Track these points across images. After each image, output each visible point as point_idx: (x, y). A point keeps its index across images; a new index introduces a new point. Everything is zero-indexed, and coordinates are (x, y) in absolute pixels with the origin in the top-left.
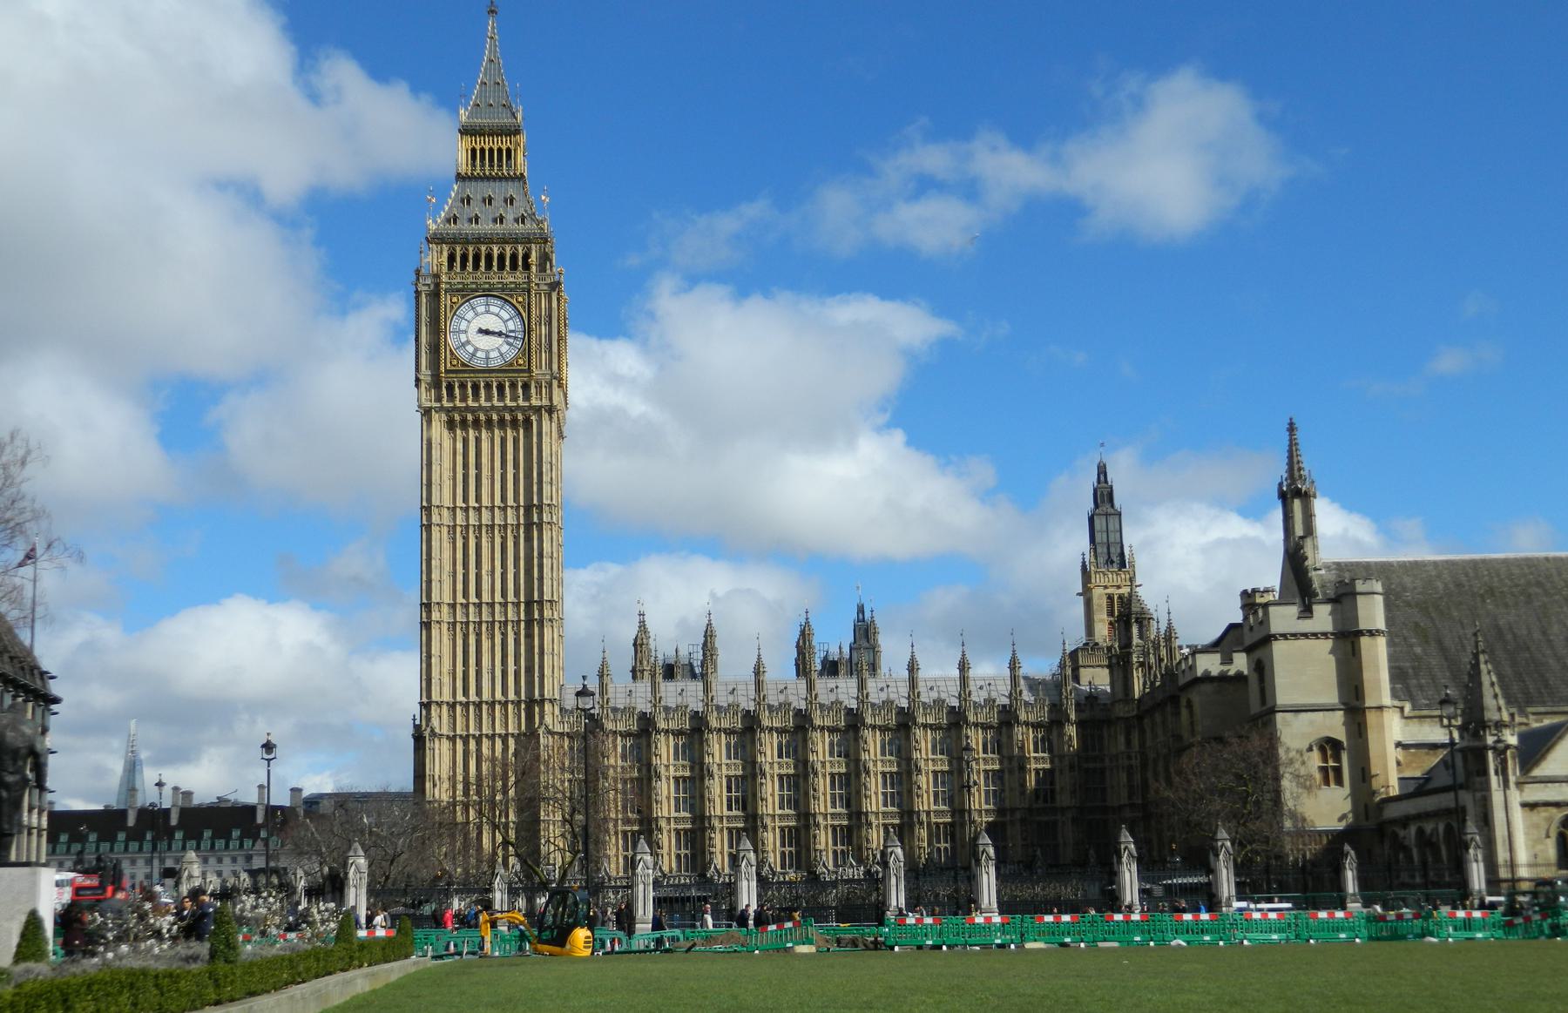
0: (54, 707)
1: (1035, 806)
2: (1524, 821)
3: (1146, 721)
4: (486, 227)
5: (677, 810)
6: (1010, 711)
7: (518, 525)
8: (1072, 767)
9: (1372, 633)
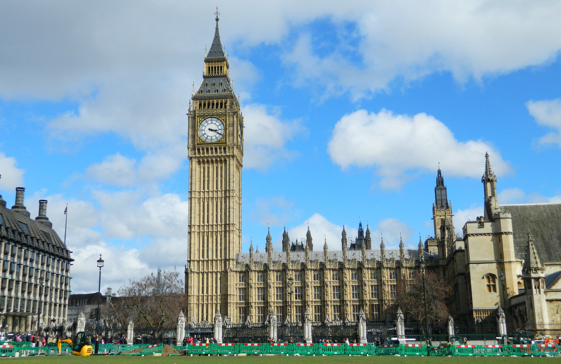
0: (71, 263)
2: (547, 307)
4: (212, 94)
5: (277, 299)
7: (222, 197)
9: (506, 233)
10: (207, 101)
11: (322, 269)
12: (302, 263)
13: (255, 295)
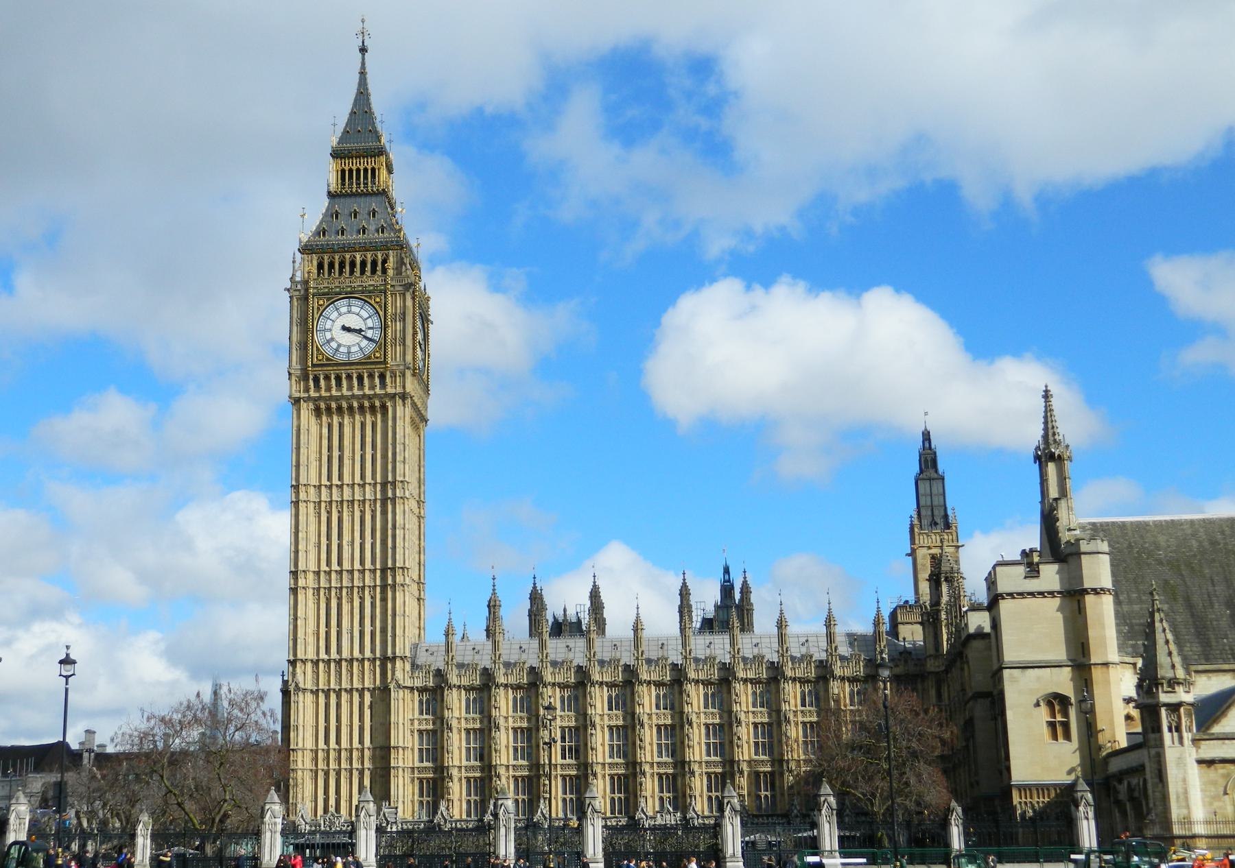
2: (1200, 778)
4: (351, 237)
5: (516, 758)
6: (826, 667)
9: (1096, 592)
10: (337, 257)
11: (629, 681)
12: (579, 668)
13: (460, 748)
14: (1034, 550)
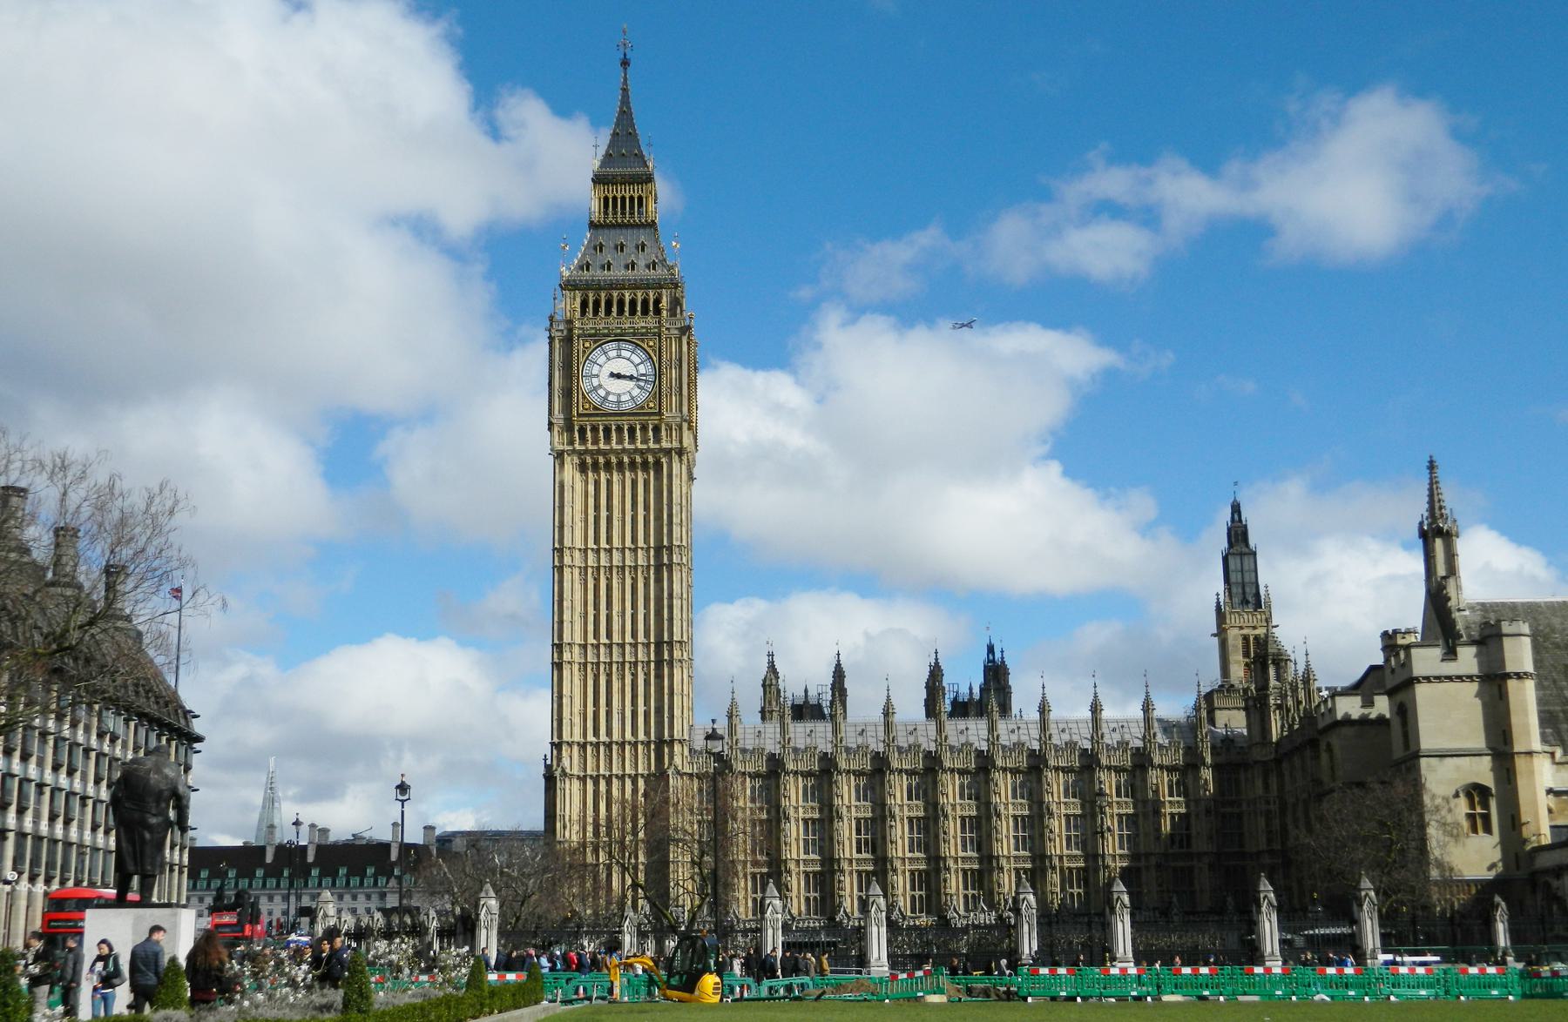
1: (1170, 851)
3: (1285, 765)
4: (618, 273)
6: (1143, 754)
8: (1208, 812)
9: (1519, 676)
14: (1412, 630)
